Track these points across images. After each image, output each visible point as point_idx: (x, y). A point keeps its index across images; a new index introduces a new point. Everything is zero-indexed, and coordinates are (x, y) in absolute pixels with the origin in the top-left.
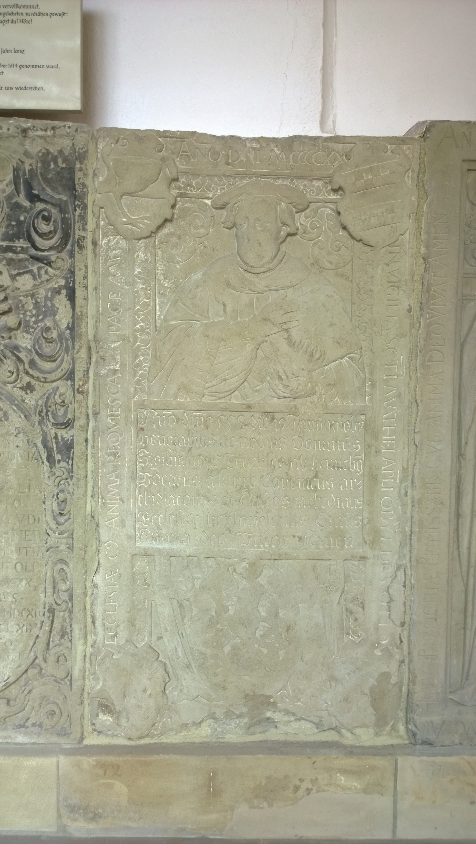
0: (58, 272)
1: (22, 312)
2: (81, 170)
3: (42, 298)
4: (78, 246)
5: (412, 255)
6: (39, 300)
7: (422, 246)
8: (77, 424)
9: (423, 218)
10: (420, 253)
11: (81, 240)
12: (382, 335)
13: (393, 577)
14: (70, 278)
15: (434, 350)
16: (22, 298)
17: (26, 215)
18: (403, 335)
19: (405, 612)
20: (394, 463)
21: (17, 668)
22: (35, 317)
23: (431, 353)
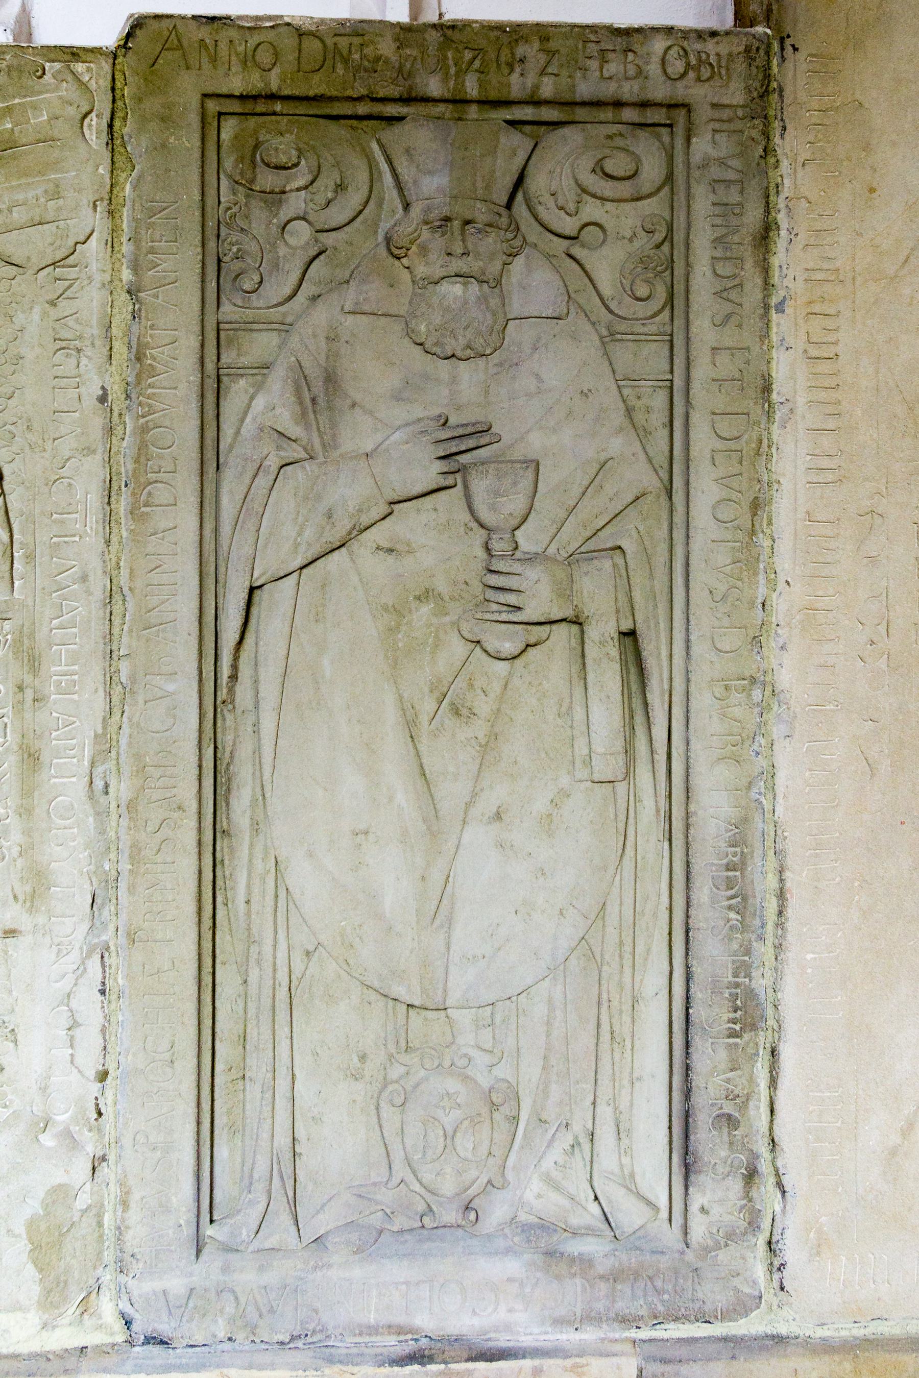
5: (104, 285)
7: (124, 267)
9: (125, 209)
10: (121, 281)
12: (45, 450)
13: (80, 971)
15: (156, 482)
18: (89, 451)
19: (105, 1048)
20: (78, 723)
23: (149, 488)
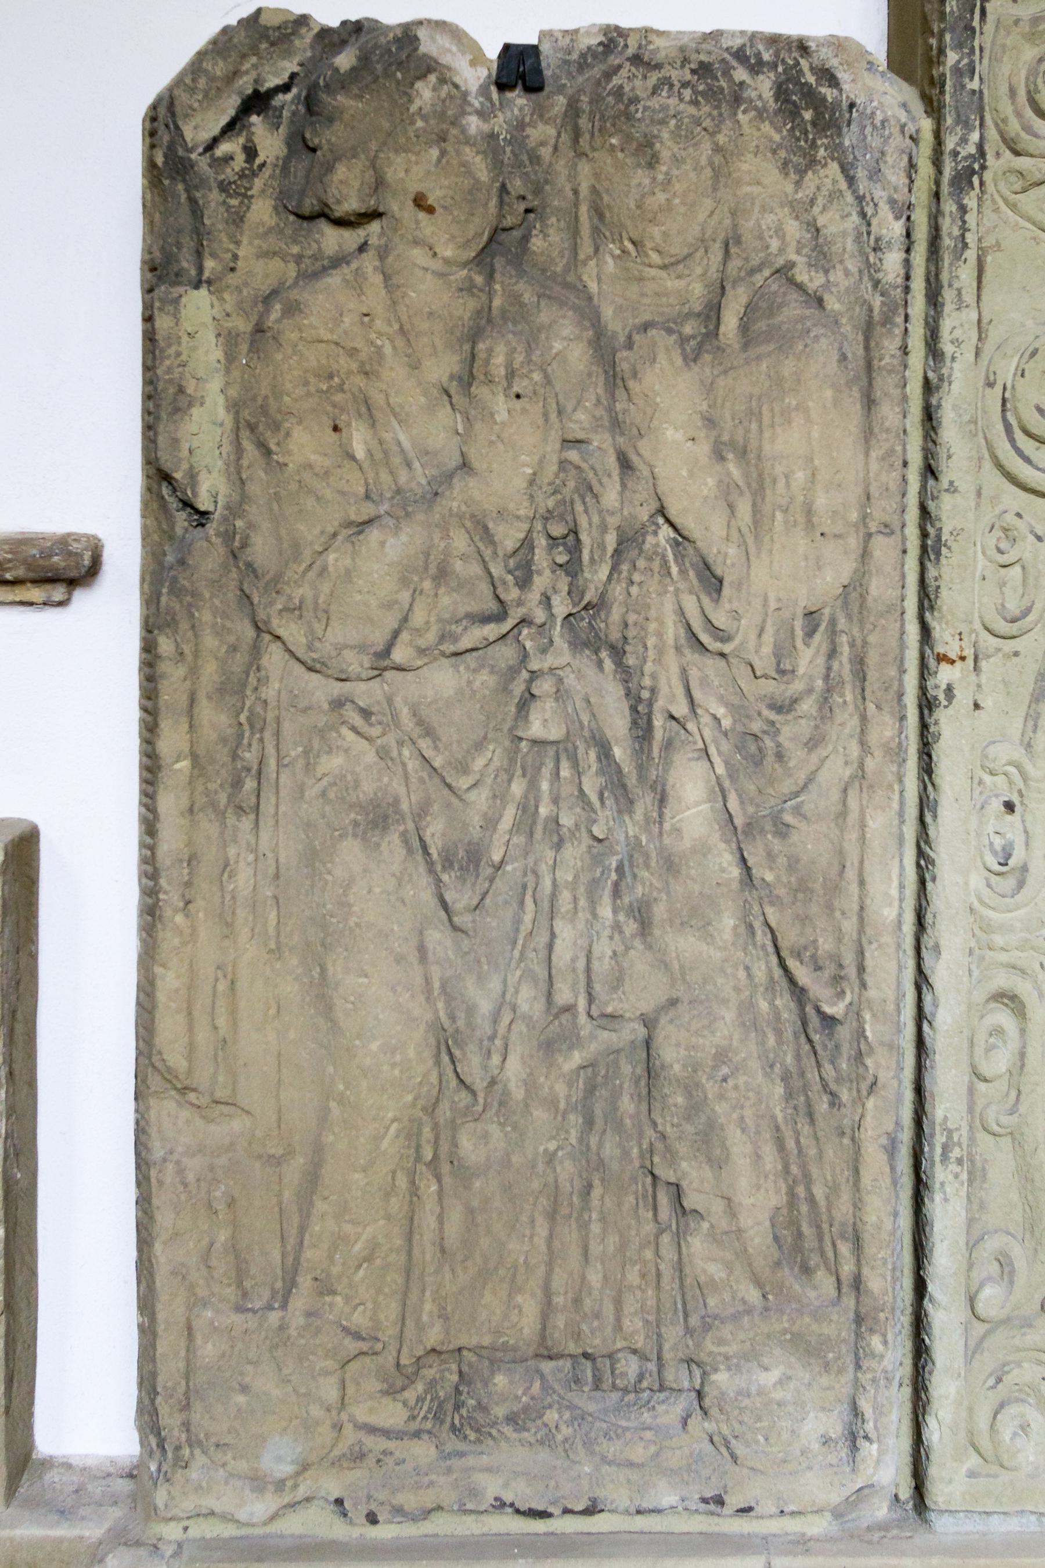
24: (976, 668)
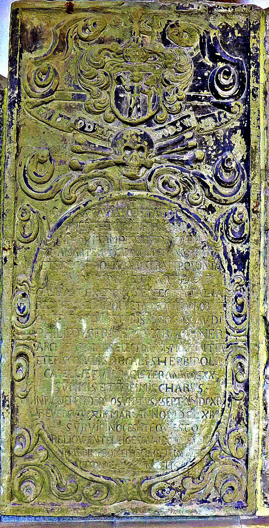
0: (234, 116)
1: (205, 148)
2: (255, 37)
3: (222, 136)
4: (252, 94)
6: (219, 138)
8: (253, 238)
11: (255, 90)
14: (245, 120)
16: (204, 136)
17: (210, 72)
21: (201, 450)
22: (216, 152)
24: (14, 252)
